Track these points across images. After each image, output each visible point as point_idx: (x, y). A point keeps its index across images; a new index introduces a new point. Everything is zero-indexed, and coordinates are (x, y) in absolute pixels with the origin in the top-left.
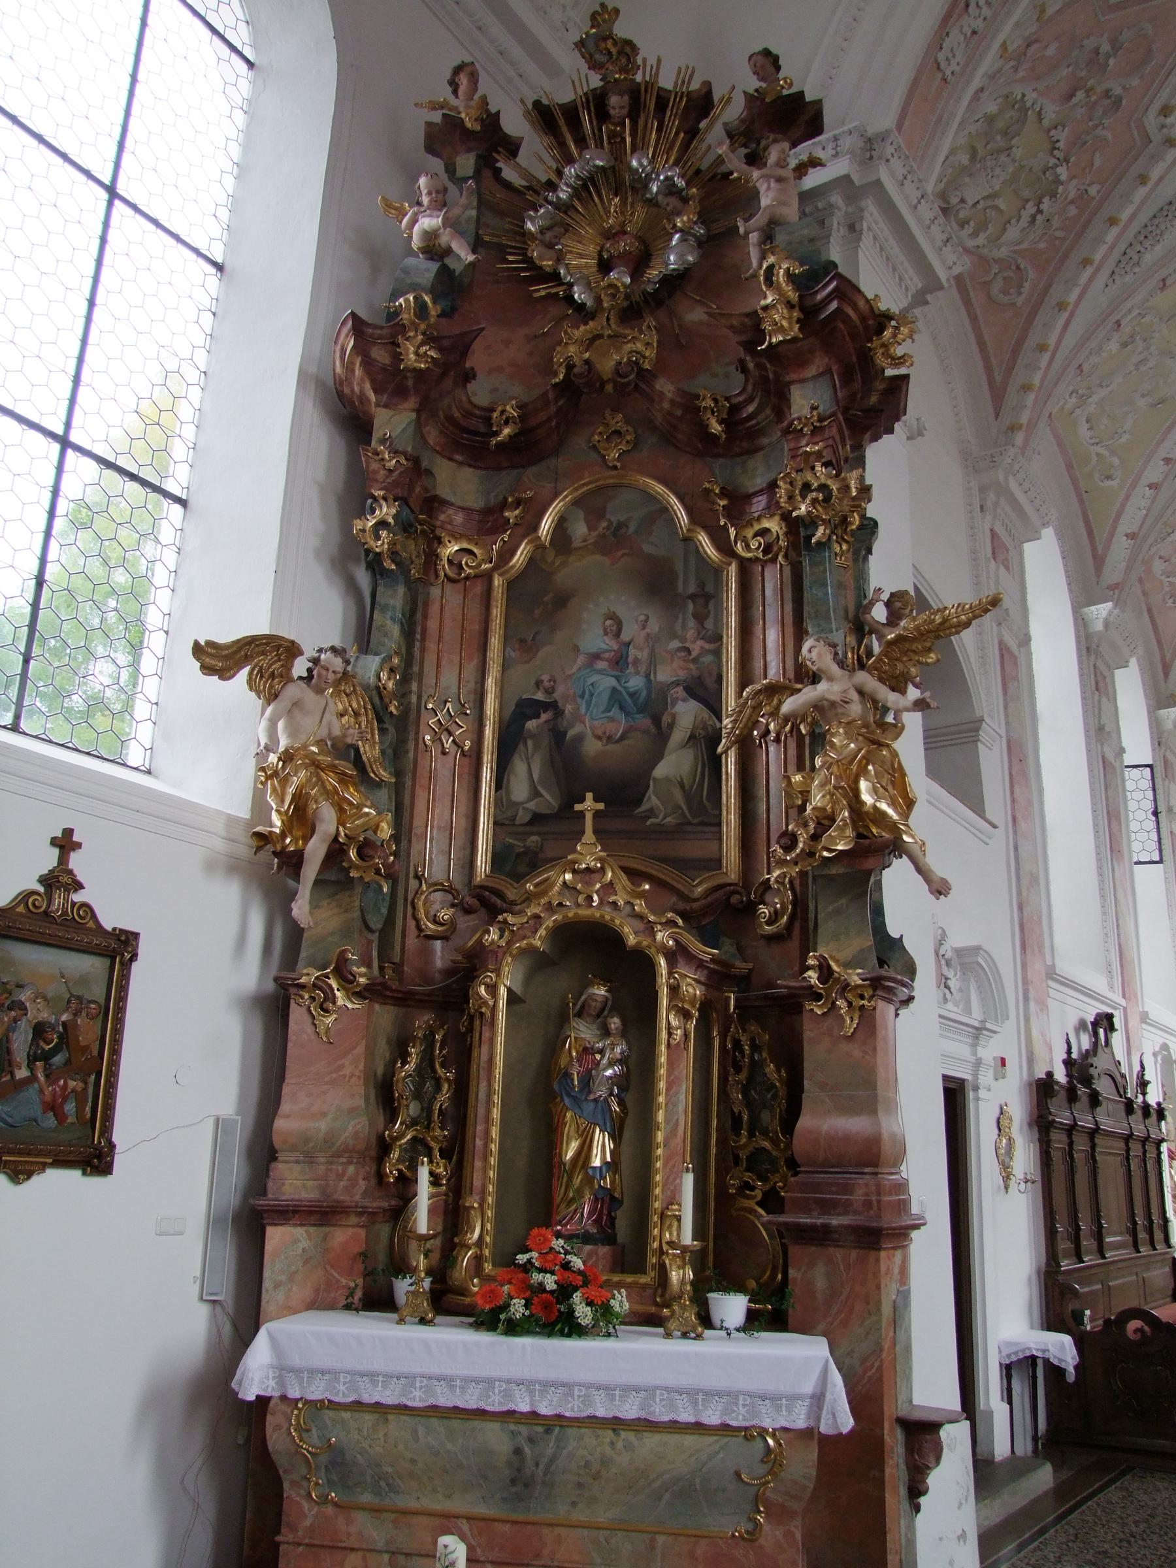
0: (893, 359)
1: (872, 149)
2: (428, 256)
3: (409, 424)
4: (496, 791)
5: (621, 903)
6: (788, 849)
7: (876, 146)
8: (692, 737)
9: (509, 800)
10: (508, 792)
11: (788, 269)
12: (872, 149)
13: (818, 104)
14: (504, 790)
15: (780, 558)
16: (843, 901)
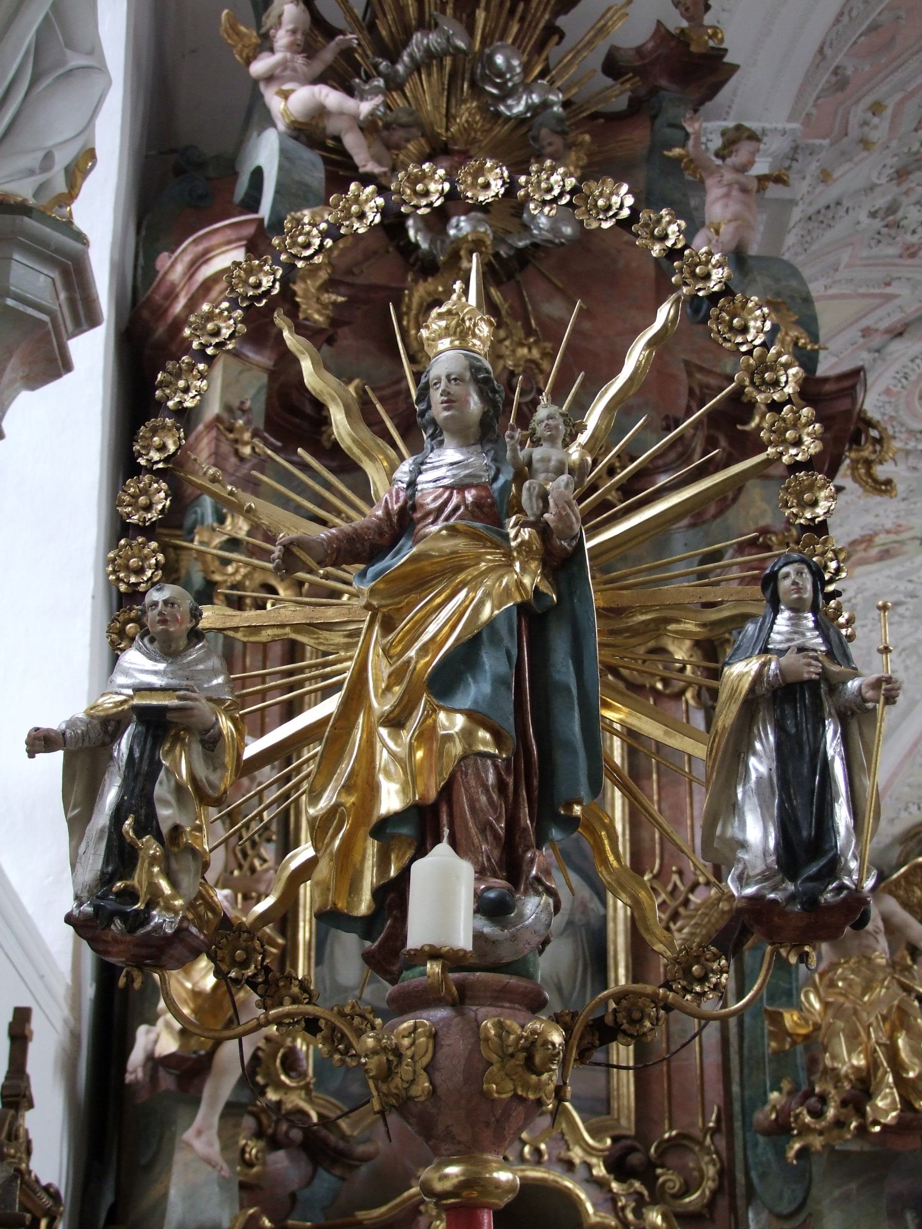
0: (875, 481)
1: (794, 159)
2: (295, 134)
3: (258, 392)
4: (319, 962)
5: (577, 1161)
6: (817, 1114)
7: (800, 157)
8: (570, 923)
9: (334, 981)
10: (332, 969)
11: (798, 339)
12: (794, 159)
13: (734, 68)
14: (325, 968)
15: (689, 695)
16: (853, 1186)
